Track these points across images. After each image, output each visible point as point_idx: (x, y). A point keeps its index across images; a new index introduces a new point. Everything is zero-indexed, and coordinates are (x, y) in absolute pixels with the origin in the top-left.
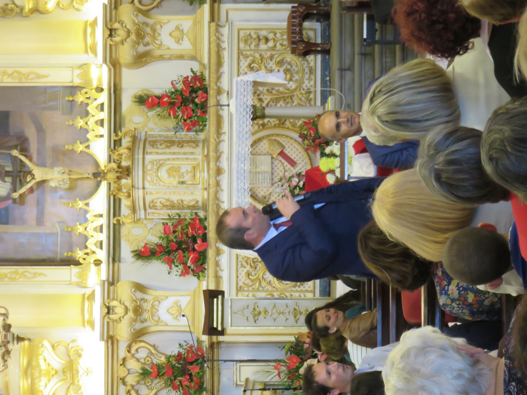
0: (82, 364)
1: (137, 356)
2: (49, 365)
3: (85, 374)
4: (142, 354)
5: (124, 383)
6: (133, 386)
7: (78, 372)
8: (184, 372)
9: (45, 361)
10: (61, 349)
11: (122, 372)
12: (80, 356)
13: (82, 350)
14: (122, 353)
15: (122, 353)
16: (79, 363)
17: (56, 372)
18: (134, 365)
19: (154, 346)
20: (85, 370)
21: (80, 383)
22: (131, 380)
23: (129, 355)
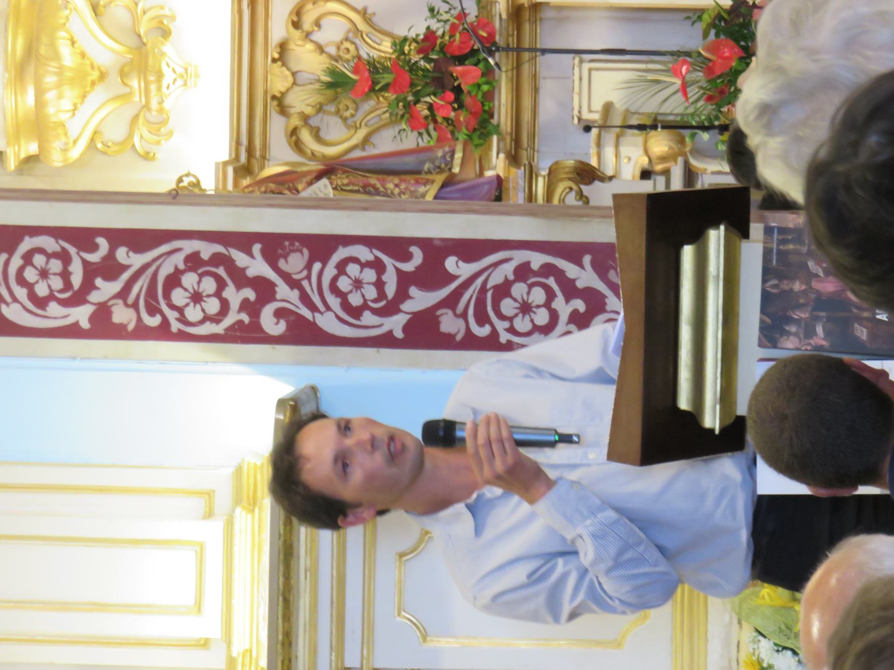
0: (172, 55)
1: (317, 36)
2: (83, 55)
3: (180, 82)
4: (332, 32)
5: (283, 110)
6: (305, 118)
7: (160, 75)
8: (440, 81)
9: (73, 43)
10: (118, 13)
11: (279, 81)
12: (165, 33)
13: (173, 18)
14: (279, 28)
15: (279, 28)
16: (163, 54)
17: (103, 76)
18: (309, 61)
19: (364, 13)
20: (179, 70)
21: (166, 105)
22: (301, 101)
23: (296, 34)
